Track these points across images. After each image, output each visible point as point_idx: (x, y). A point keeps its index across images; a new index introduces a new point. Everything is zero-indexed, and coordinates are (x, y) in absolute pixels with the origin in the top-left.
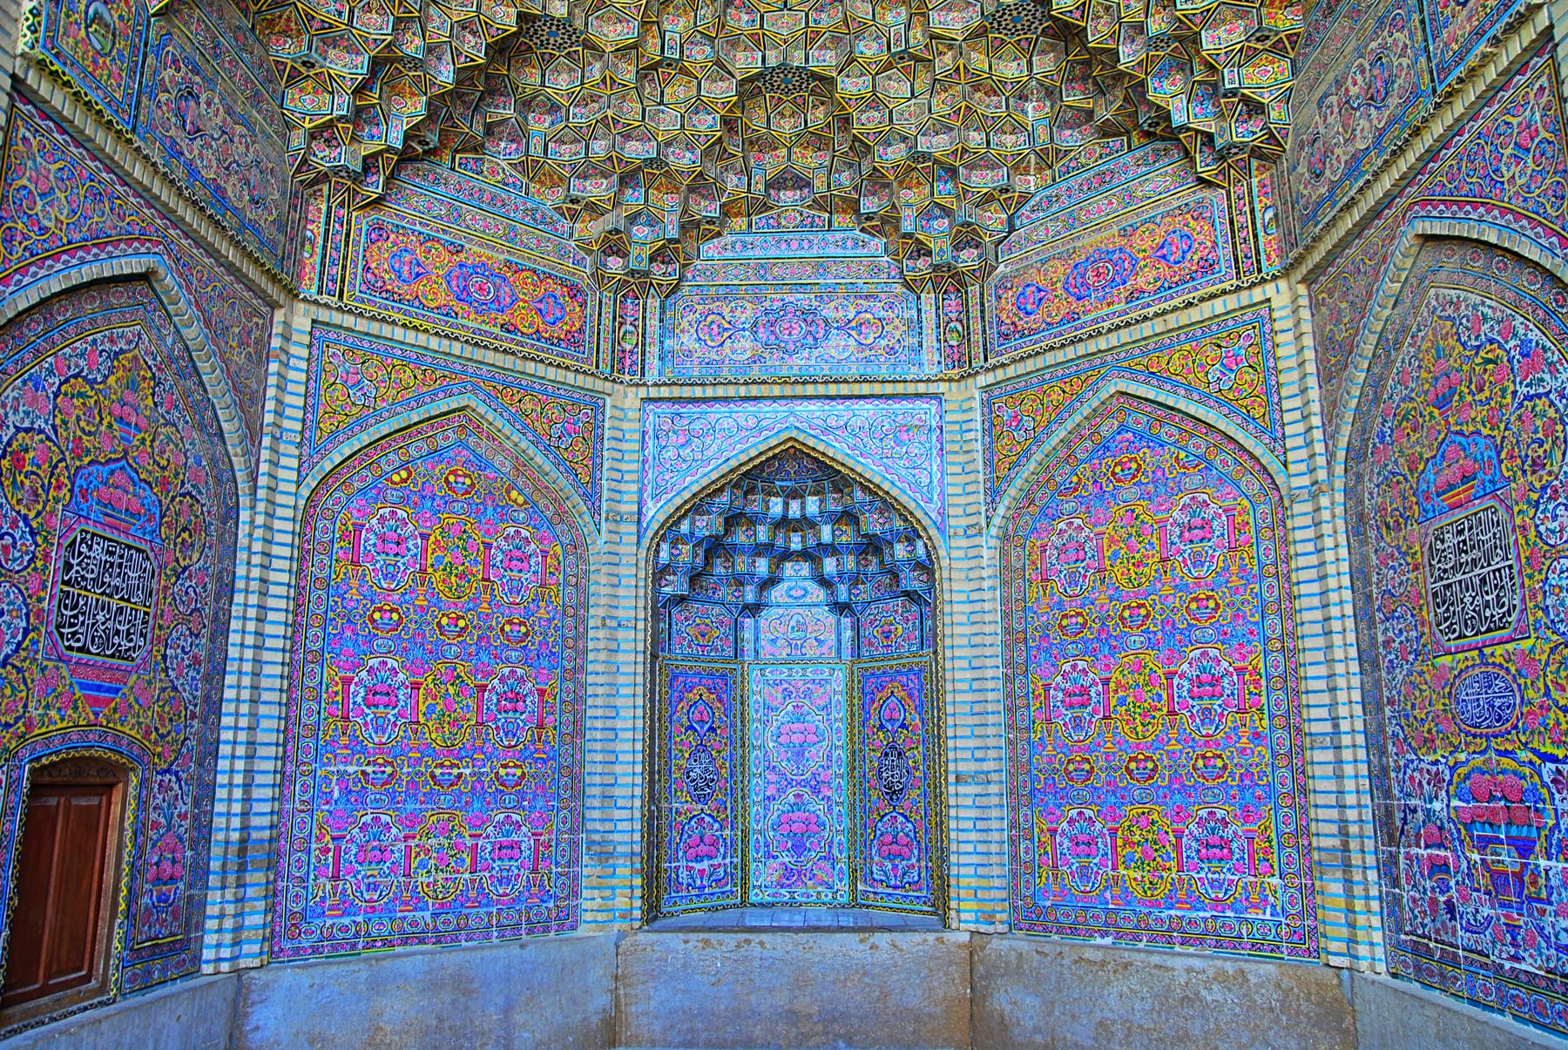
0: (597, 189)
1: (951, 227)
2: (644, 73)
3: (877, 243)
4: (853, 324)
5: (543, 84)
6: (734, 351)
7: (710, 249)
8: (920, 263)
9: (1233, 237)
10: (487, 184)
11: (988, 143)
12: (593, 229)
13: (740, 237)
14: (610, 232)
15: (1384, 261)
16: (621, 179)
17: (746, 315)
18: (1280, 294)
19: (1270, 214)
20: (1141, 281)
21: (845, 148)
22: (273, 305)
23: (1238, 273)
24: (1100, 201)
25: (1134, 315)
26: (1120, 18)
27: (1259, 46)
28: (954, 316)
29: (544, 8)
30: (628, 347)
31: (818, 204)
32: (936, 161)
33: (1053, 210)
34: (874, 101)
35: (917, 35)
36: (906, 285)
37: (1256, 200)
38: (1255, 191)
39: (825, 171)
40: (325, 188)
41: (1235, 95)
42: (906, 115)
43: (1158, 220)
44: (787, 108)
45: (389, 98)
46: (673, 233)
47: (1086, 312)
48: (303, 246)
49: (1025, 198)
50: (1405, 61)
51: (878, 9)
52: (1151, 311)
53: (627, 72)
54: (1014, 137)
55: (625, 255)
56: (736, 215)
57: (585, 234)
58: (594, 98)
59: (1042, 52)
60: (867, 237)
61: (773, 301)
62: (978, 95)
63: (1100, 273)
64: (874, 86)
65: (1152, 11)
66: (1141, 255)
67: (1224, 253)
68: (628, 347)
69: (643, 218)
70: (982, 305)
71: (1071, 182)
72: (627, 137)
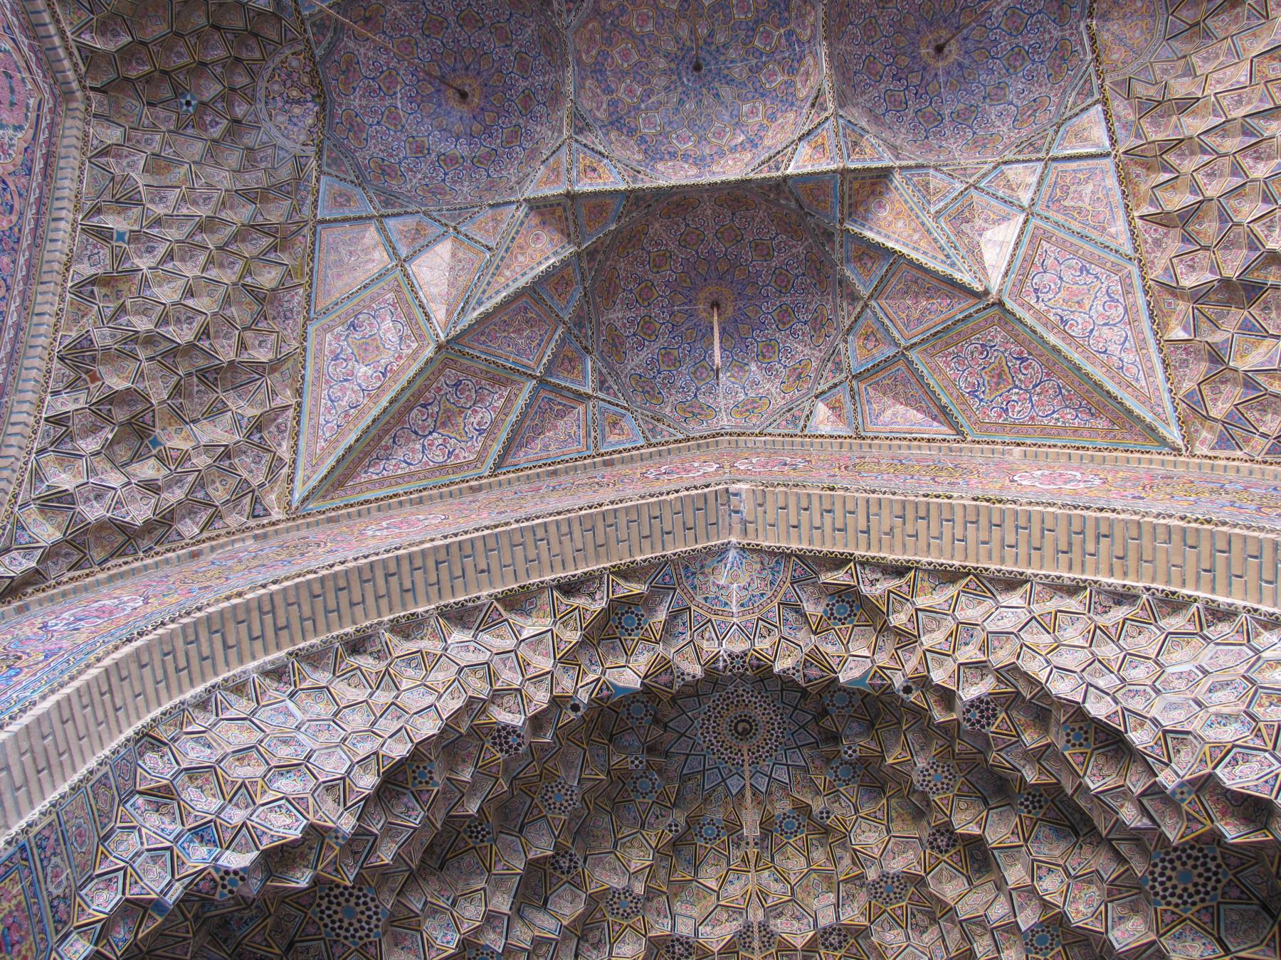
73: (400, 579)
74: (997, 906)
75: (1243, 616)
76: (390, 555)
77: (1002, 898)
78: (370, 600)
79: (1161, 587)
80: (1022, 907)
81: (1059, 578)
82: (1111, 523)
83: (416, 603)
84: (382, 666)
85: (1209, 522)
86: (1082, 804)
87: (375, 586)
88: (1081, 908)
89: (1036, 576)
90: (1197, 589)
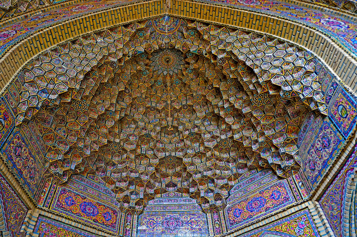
0: (123, 185)
1: (213, 195)
2: (136, 157)
3: (194, 201)
4: (189, 222)
5: (112, 159)
6: (157, 230)
7: (151, 202)
8: (206, 205)
9: (292, 191)
10: (96, 183)
11: (221, 173)
12: (121, 195)
13: (159, 199)
14: (125, 196)
15: (344, 188)
16: (129, 182)
17: (161, 219)
18: (310, 205)
19: (300, 184)
20: (268, 205)
21: (185, 175)
22: (29, 209)
23: (296, 200)
24: (252, 185)
25: (269, 215)
26: (251, 139)
27: (287, 142)
28: (216, 219)
29: (114, 140)
30: (128, 229)
31: (178, 191)
32: (209, 177)
33: (240, 189)
34: (192, 164)
35: (202, 148)
36: (203, 211)
37: (296, 181)
38: (295, 178)
39: (180, 182)
40: (52, 178)
41: (284, 154)
42: (200, 167)
43: (269, 188)
44: (171, 167)
45: (73, 157)
46: (142, 197)
47: (254, 215)
48: (42, 193)
49: (232, 187)
50: (332, 135)
51: (192, 143)
52: (273, 213)
53: (133, 156)
54: (227, 171)
55: (128, 202)
56: (158, 193)
57: (119, 197)
58: (124, 162)
59: (232, 151)
60: (192, 199)
61: (167, 216)
62: (217, 161)
63: (255, 204)
64: (192, 160)
65: (259, 136)
66: (267, 198)
67: (290, 195)
68: (128, 229)
69: (134, 193)
70: (224, 216)
71: (243, 182)
72: (131, 172)
73: (84, 24)
74: (220, 102)
75: (286, 44)
76: (80, 18)
77: (222, 101)
78: (76, 30)
79: (269, 34)
80: (226, 103)
81: (245, 29)
82: (260, 16)
83: (88, 30)
84: (81, 47)
85: (284, 19)
86: (241, 83)
87: (77, 26)
88: (238, 104)
89: (240, 28)
90: (277, 35)
